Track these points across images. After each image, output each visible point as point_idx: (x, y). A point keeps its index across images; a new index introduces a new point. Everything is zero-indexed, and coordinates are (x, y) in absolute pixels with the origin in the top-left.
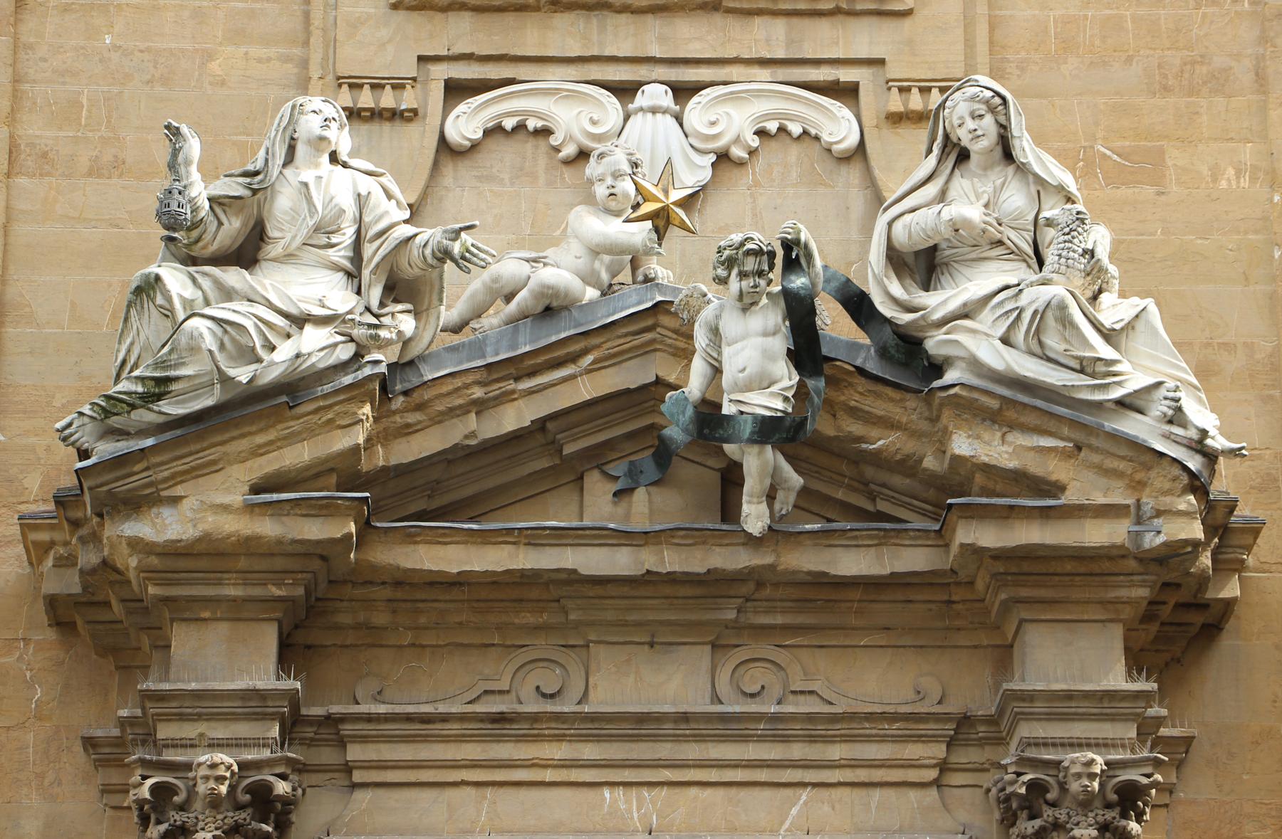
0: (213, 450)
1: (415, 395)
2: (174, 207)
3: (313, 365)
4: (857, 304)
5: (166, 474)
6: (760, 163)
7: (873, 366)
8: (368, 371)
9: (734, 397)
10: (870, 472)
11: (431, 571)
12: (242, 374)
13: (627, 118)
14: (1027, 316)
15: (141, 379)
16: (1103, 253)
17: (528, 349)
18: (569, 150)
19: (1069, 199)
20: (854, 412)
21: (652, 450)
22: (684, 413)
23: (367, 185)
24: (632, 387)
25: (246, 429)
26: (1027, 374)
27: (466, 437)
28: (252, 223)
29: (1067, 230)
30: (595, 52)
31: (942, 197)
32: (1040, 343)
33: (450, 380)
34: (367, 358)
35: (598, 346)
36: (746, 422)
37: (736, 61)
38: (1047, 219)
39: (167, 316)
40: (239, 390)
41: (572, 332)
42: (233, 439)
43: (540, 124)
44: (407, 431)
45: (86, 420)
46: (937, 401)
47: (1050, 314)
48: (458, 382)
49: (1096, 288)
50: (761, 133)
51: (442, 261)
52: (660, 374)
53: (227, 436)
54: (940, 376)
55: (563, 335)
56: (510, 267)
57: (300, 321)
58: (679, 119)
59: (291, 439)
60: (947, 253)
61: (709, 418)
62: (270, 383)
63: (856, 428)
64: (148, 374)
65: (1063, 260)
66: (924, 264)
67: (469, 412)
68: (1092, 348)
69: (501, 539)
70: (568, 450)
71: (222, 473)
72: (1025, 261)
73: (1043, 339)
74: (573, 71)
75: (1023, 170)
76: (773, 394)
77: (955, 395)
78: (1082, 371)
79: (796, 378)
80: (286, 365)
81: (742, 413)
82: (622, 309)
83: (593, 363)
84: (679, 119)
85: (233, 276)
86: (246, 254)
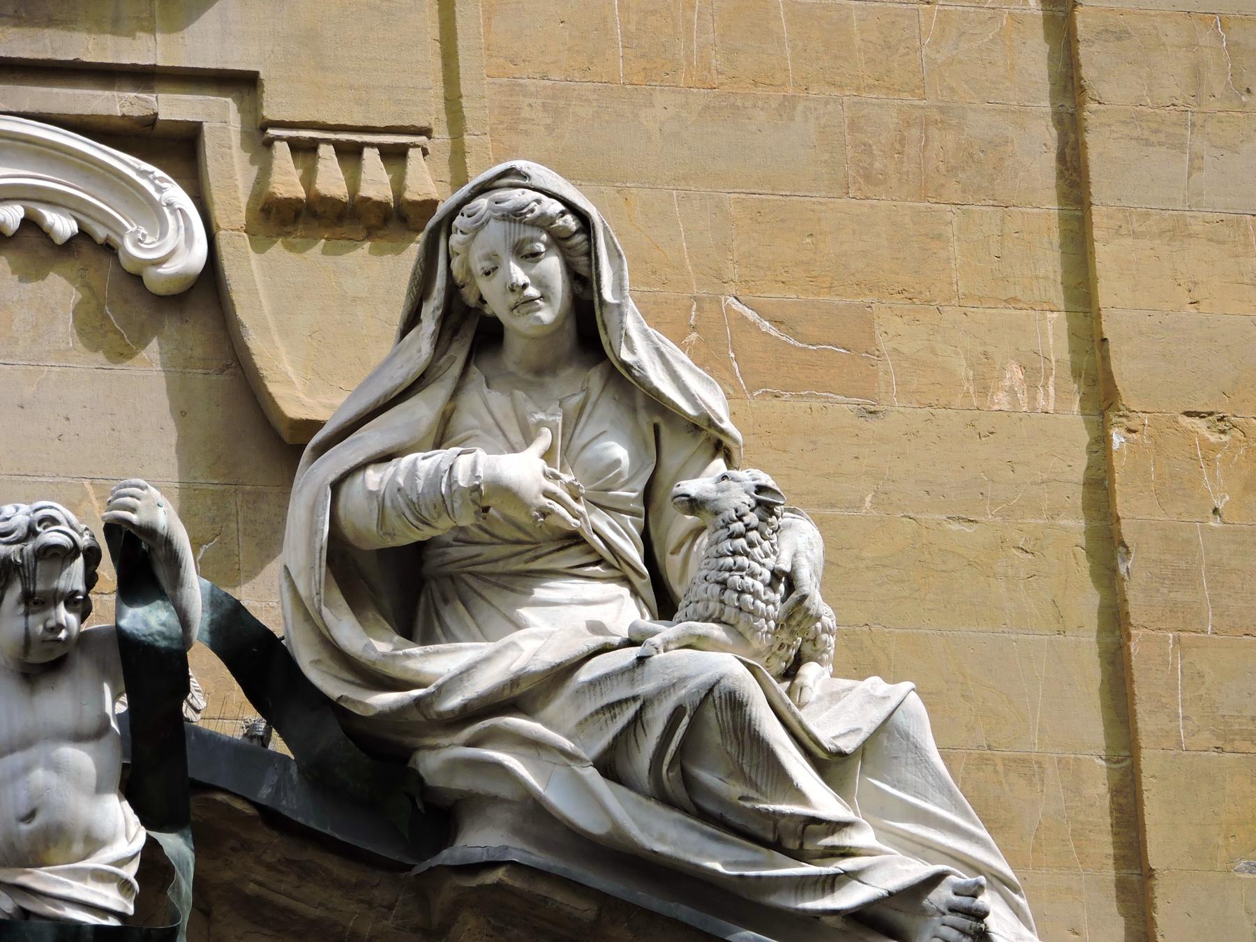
7: (295, 806)
16: (809, 582)
26: (659, 847)
32: (688, 781)
60: (456, 552)
66: (411, 578)
68: (799, 796)
72: (625, 580)
76: (101, 876)
77: (499, 886)
81: (26, 914)
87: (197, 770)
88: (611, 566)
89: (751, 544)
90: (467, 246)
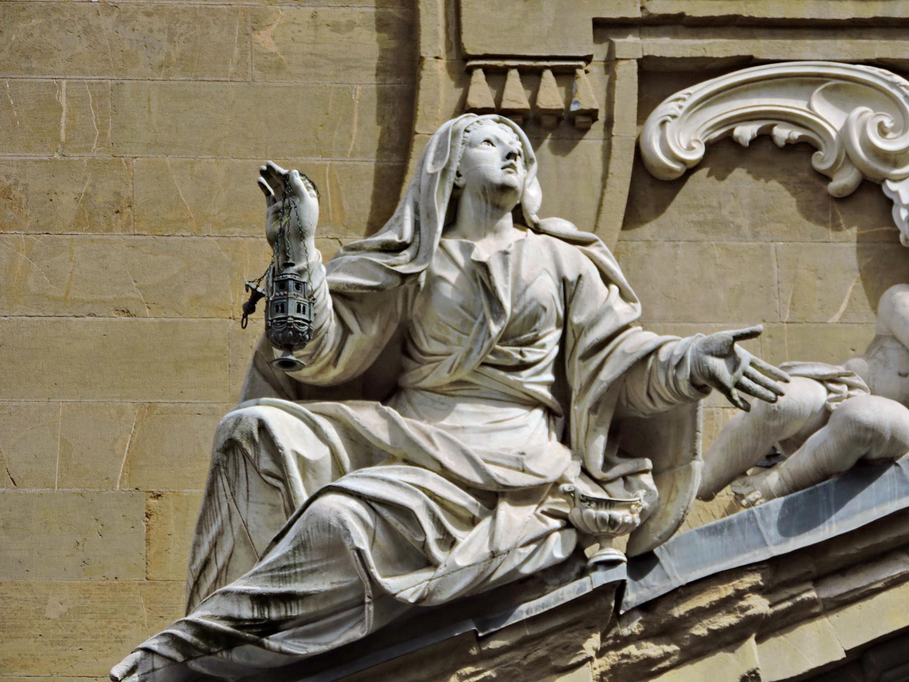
1: (659, 609)
2: (292, 311)
3: (515, 571)
8: (600, 578)
12: (407, 586)
18: (844, 180)
23: (575, 262)
28: (394, 327)
40: (398, 613)
43: (796, 133)
45: (158, 663)
48: (726, 590)
51: (703, 390)
56: (803, 393)
57: (490, 496)
67: (743, 638)
80: (475, 572)
85: (368, 417)
86: (383, 382)
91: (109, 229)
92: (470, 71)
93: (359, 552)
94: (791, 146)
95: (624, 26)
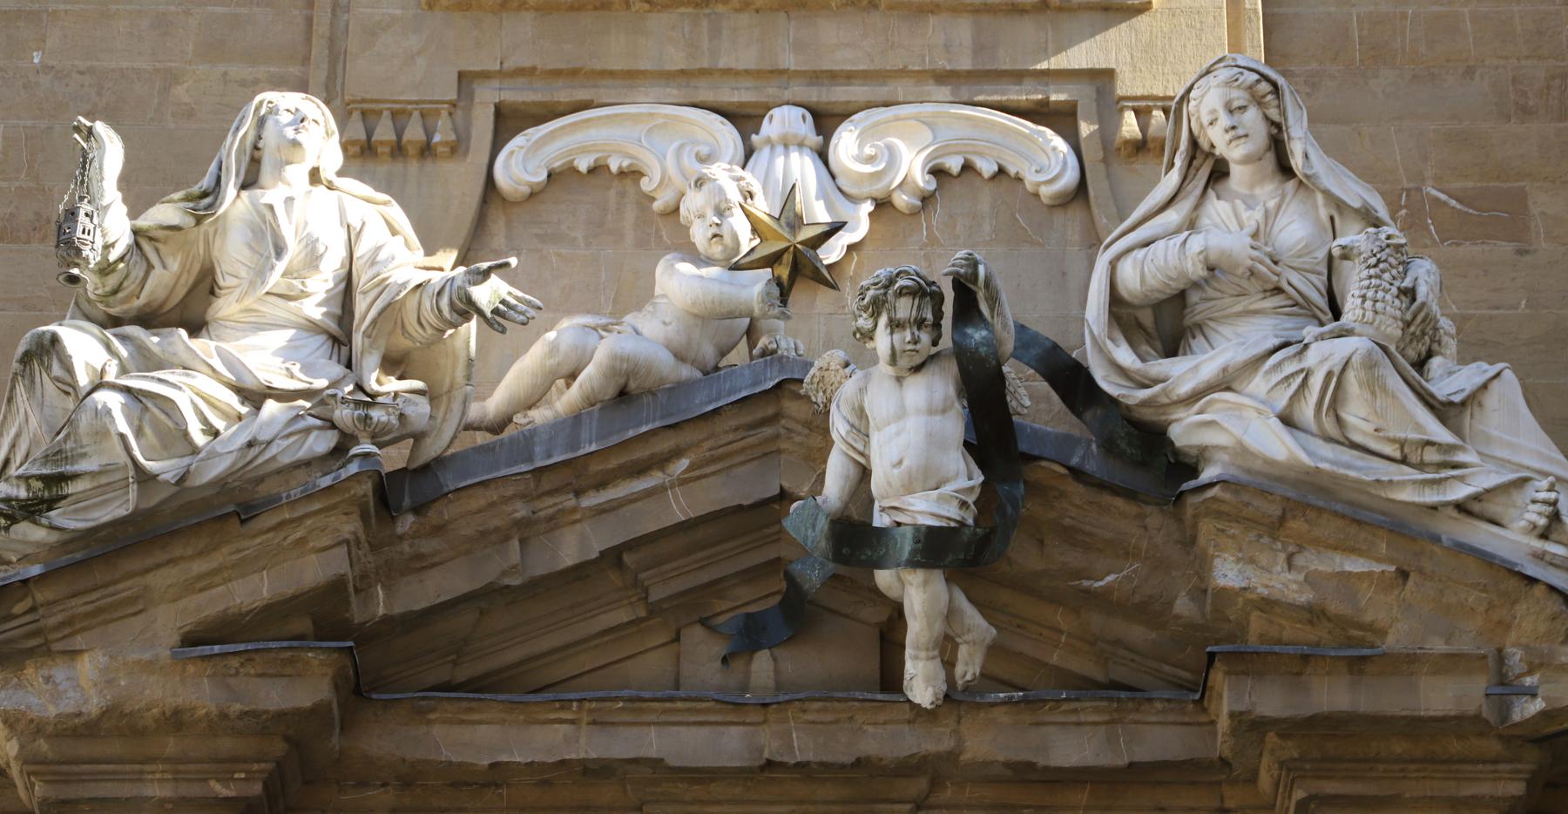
0: (128, 583)
3: (274, 458)
4: (1071, 380)
5: (60, 618)
6: (939, 213)
9: (887, 503)
10: (1096, 621)
11: (450, 763)
13: (749, 152)
14: (1316, 382)
15: (26, 478)
17: (594, 448)
19: (1377, 223)
20: (1070, 535)
21: (778, 598)
22: (814, 526)
24: (746, 502)
25: (178, 551)
27: (504, 573)
28: (197, 268)
29: (1373, 261)
30: (705, 63)
31: (1191, 225)
32: (1339, 420)
33: (480, 491)
34: (355, 450)
35: (698, 444)
36: (904, 536)
37: (902, 73)
38: (1343, 247)
39: (67, 393)
41: (658, 424)
42: (158, 566)
44: (420, 564)
46: (1189, 512)
47: (1351, 376)
48: (493, 494)
49: (1424, 349)
50: (938, 172)
52: (786, 485)
53: (149, 561)
54: (1196, 477)
55: (644, 429)
58: (823, 155)
59: (242, 568)
61: (855, 536)
62: (211, 484)
63: (1074, 558)
64: (34, 471)
65: (1368, 304)
66: (1166, 322)
69: (553, 716)
70: (656, 594)
71: (142, 616)
72: (1315, 317)
73: (1344, 415)
74: (673, 92)
75: (1306, 186)
76: (941, 499)
77: (1214, 499)
78: (1404, 461)
79: (979, 478)
81: (899, 524)
82: (730, 393)
83: (690, 468)
84: (823, 155)
87: (1023, 446)
88: (1302, 307)
89: (1383, 271)
90: (1197, 106)
91: (28, 242)
92: (350, 113)
93: (122, 436)
94: (622, 173)
95: (485, 75)
